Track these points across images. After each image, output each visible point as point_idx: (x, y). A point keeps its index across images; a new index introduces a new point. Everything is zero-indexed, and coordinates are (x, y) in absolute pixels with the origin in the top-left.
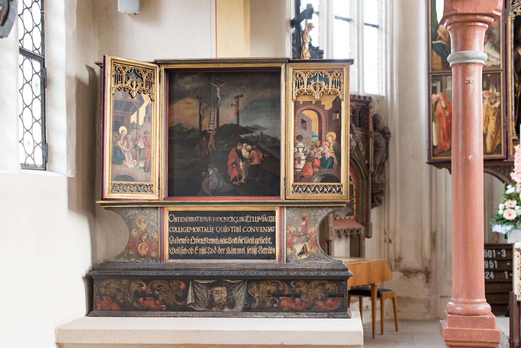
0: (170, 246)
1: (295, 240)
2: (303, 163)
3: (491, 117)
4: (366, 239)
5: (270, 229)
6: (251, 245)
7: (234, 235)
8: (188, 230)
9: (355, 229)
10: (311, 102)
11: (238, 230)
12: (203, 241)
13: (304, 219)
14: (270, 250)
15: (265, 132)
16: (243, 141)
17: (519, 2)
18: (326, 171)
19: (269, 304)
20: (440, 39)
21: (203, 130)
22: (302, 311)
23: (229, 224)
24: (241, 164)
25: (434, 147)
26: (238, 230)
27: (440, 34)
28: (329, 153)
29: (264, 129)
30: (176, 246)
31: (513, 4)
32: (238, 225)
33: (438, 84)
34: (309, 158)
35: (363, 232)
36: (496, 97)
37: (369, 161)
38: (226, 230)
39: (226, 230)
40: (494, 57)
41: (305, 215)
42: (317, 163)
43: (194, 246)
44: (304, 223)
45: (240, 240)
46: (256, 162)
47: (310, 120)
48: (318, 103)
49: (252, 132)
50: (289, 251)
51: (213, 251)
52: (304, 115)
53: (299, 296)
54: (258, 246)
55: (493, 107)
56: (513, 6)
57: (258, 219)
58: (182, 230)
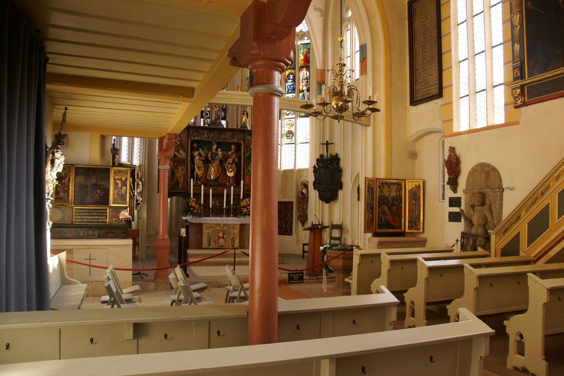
1: (113, 217)
2: (116, 195)
3: (182, 177)
4: (133, 222)
5: (106, 214)
6: (100, 219)
7: (95, 216)
8: (81, 214)
10: (119, 178)
11: (96, 214)
12: (85, 217)
13: (116, 211)
14: (105, 220)
15: (105, 186)
16: (98, 189)
18: (122, 198)
19: (105, 235)
21: (86, 184)
22: (115, 237)
23: (94, 213)
24: (97, 195)
26: (96, 214)
29: (104, 185)
30: (77, 219)
31: (191, 136)
32: (96, 213)
34: (118, 194)
35: (131, 219)
36: (184, 169)
37: (135, 191)
38: (92, 214)
39: (92, 214)
40: (183, 154)
41: (116, 210)
42: (120, 195)
43: (82, 219)
44: (116, 213)
45: (96, 217)
46: (102, 195)
47: (118, 183)
48: (121, 178)
49: (101, 186)
50: (111, 221)
51: (88, 220)
52: (117, 182)
53: (114, 233)
54: (102, 219)
55: (182, 173)
57: (102, 211)
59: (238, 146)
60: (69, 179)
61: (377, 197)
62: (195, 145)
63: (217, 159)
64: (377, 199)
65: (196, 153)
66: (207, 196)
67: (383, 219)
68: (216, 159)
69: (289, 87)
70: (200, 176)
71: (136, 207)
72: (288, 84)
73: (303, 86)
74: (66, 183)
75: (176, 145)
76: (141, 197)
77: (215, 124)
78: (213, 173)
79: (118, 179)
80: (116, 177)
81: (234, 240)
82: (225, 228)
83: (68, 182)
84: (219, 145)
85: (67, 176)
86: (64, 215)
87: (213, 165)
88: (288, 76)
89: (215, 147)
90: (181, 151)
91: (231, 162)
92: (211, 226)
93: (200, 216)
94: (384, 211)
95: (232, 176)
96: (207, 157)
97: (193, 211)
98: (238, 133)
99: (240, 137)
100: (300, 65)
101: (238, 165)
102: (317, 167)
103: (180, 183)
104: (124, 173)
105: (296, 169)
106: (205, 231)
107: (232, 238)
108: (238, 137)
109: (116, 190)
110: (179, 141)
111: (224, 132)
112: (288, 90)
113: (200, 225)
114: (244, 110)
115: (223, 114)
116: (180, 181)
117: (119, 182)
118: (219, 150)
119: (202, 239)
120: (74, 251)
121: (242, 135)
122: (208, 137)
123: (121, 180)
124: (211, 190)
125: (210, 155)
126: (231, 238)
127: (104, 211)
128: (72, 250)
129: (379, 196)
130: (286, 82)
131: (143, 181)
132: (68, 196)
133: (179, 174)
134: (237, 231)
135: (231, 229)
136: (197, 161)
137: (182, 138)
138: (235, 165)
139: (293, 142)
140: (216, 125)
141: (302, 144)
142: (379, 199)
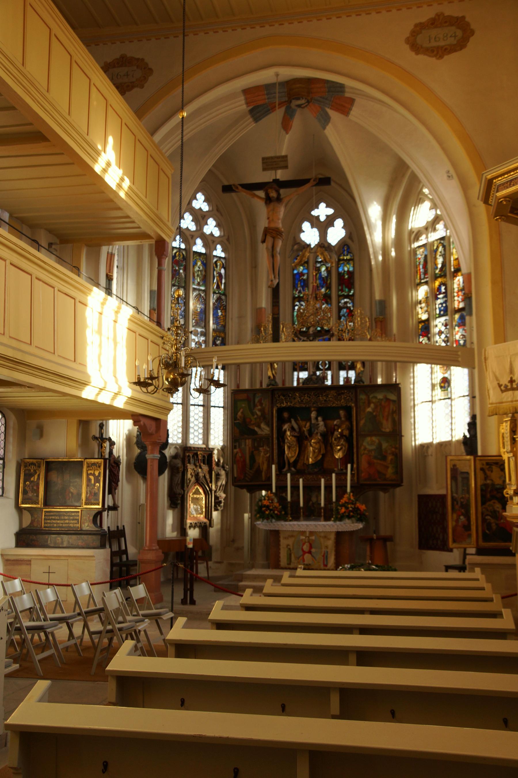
0: (44, 523)
2: (89, 494)
4: (211, 528)
6: (71, 523)
9: (203, 522)
11: (66, 518)
13: (89, 514)
20: (239, 420)
24: (70, 494)
25: (235, 478)
27: (238, 417)
28: (96, 491)
30: (46, 523)
32: (67, 516)
33: (237, 444)
40: (266, 430)
43: (52, 523)
44: (88, 516)
54: (73, 523)
55: (266, 456)
58: (48, 518)
59: (348, 410)
60: (39, 476)
61: (479, 488)
62: (286, 415)
63: (317, 433)
64: (479, 492)
65: (286, 427)
66: (295, 488)
67: (493, 525)
68: (315, 432)
69: (440, 306)
70: (292, 460)
71: (215, 506)
72: (439, 301)
73: (459, 302)
74: (35, 480)
75: (256, 416)
76: (224, 493)
78: (311, 456)
79: (91, 474)
80: (89, 472)
81: (327, 557)
82: (313, 538)
83: (37, 479)
84: (320, 412)
85: (36, 473)
86: (33, 519)
87: (312, 443)
88: (439, 289)
89: (313, 415)
90: (263, 425)
91: (339, 436)
92: (292, 534)
93: (279, 518)
94: (495, 511)
95: (341, 457)
96: (301, 432)
97: (264, 513)
98: (346, 391)
99: (350, 396)
100: (454, 268)
101: (349, 440)
102: (468, 436)
103: (261, 472)
104: (96, 466)
105: (454, 440)
106: (283, 542)
107: (324, 554)
108: (346, 398)
109: (88, 488)
110: (260, 410)
112: (440, 311)
113: (276, 533)
116: (263, 469)
117: (92, 477)
118: (320, 419)
119: (279, 553)
120: (32, 562)
121: (352, 394)
123: (94, 475)
124: (301, 480)
125: (309, 428)
126: (323, 554)
127: (76, 514)
128: (30, 561)
129: (481, 486)
130: (437, 298)
131: (227, 470)
132: (38, 496)
133: (261, 459)
134: (331, 543)
135: (322, 540)
136: (288, 439)
137: (264, 405)
138: (344, 440)
139: (449, 396)
141: (463, 398)
142: (482, 490)
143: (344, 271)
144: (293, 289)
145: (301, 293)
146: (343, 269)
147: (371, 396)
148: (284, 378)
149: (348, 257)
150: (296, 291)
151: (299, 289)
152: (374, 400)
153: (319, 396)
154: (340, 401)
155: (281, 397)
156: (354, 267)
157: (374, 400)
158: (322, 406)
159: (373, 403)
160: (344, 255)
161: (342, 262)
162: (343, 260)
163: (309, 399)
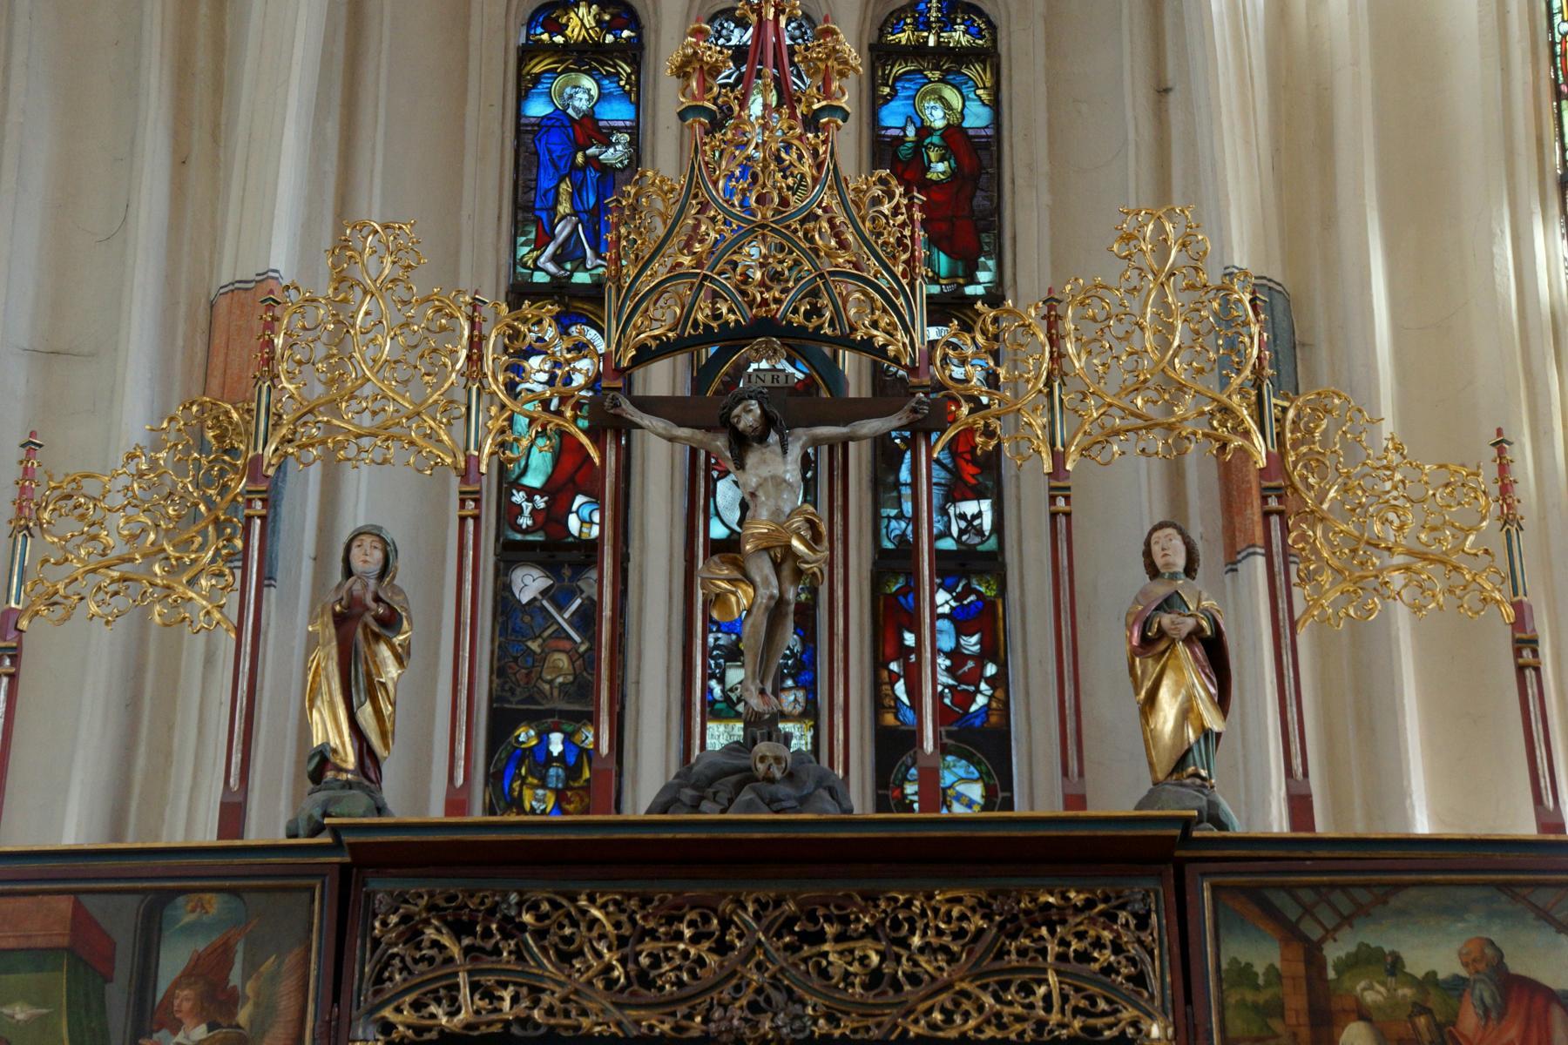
17: (410, 973)
56: (376, 993)
77: (739, 787)
99: (1117, 948)
108: (1083, 957)
111: (871, 898)
114: (1161, 590)
115: (976, 792)
121: (1143, 922)
122: (644, 979)
137: (243, 1016)
140: (747, 795)
143: (924, 131)
144: (517, 229)
145: (581, 264)
146: (915, 118)
147: (1334, 952)
148: (460, 781)
149: (959, 36)
150: (540, 244)
151: (562, 231)
152: (1373, 994)
153: (820, 937)
154: (1026, 989)
155: (430, 933)
156: (995, 105)
157: (1373, 994)
158: (846, 1027)
159: (1363, 1014)
160: (923, 24)
161: (898, 69)
162: (918, 51)
163: (712, 960)
